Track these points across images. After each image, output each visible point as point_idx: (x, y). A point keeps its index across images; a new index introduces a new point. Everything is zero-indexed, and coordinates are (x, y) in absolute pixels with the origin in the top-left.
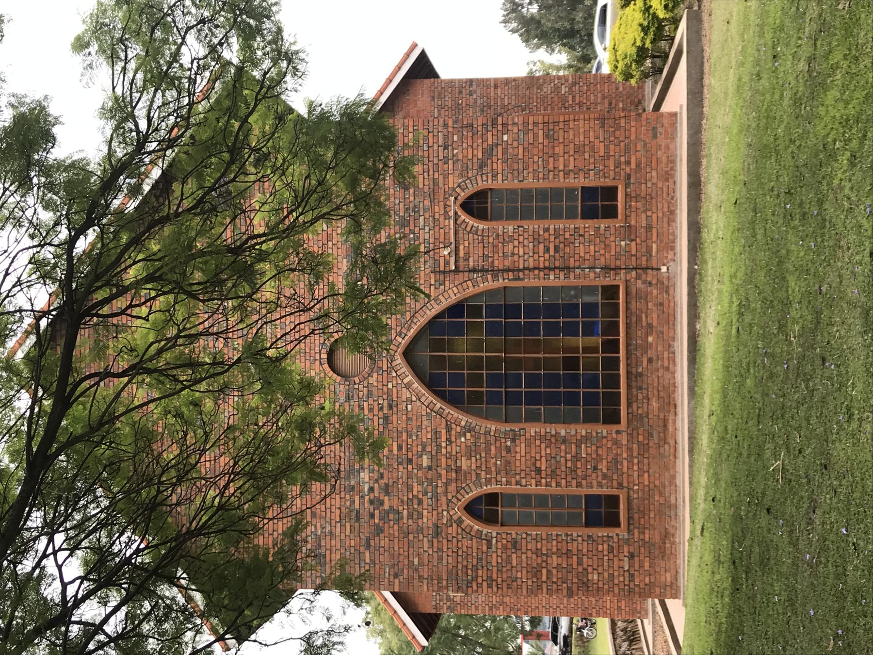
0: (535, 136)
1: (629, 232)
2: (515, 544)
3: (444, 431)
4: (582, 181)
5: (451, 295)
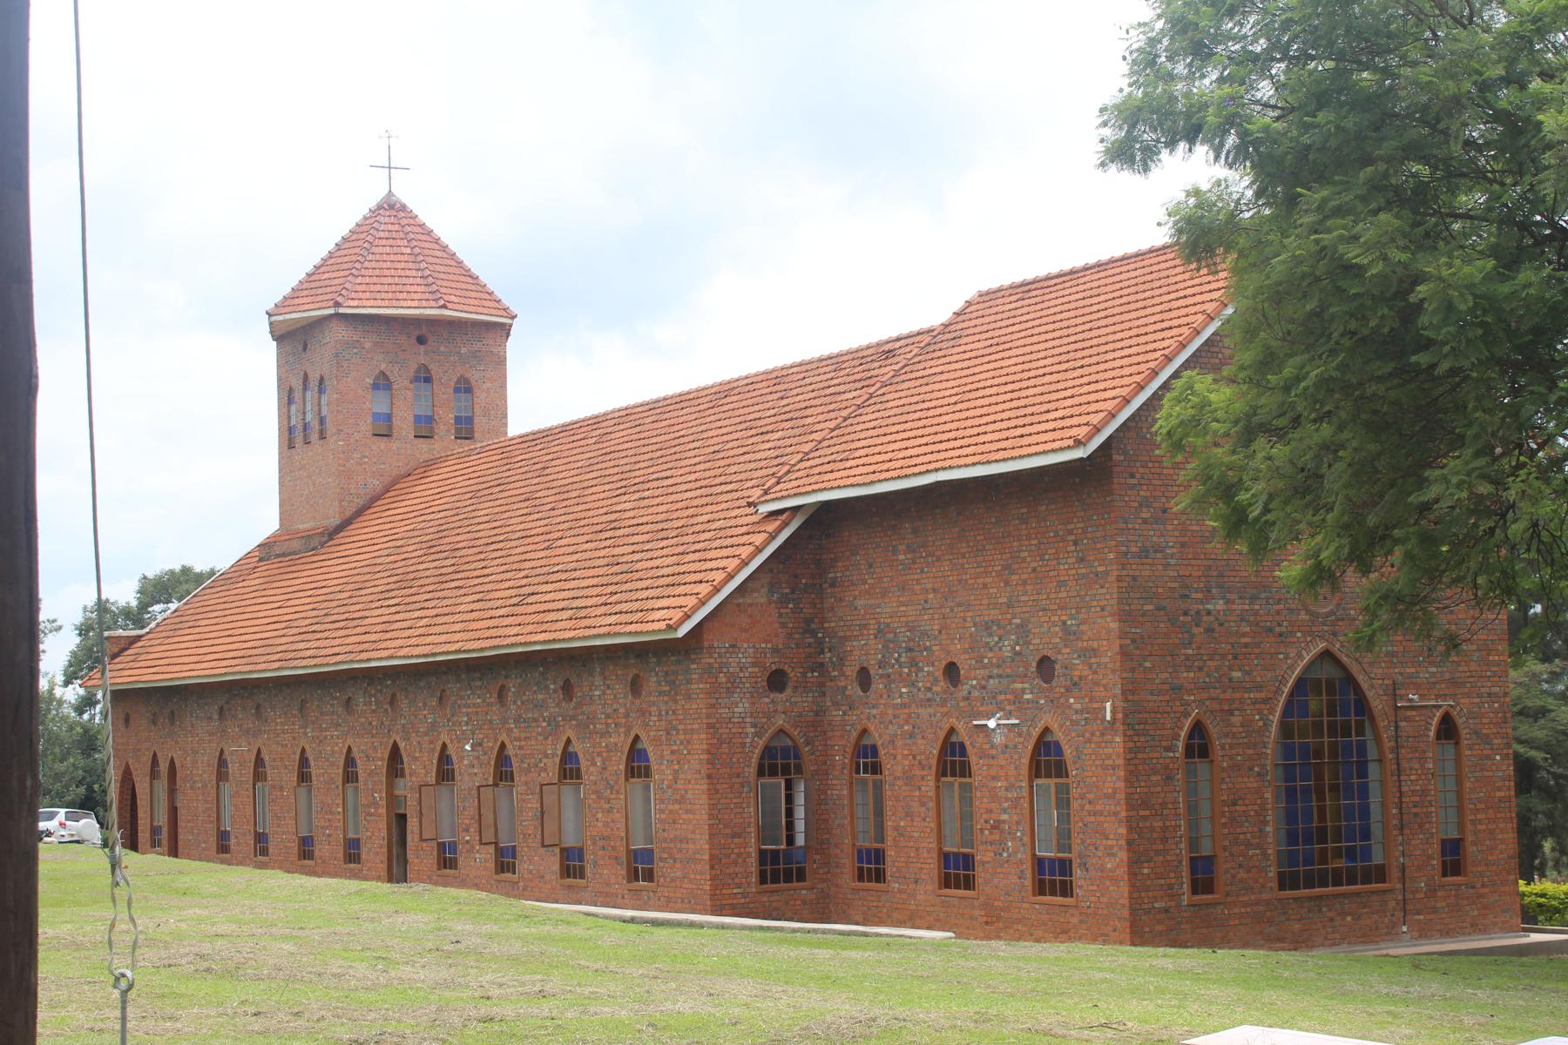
0: (1499, 789)
1: (1431, 892)
2: (1169, 779)
3: (1263, 695)
4: (1470, 838)
5: (1377, 703)
